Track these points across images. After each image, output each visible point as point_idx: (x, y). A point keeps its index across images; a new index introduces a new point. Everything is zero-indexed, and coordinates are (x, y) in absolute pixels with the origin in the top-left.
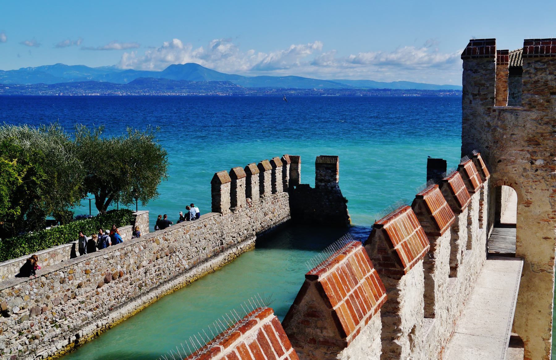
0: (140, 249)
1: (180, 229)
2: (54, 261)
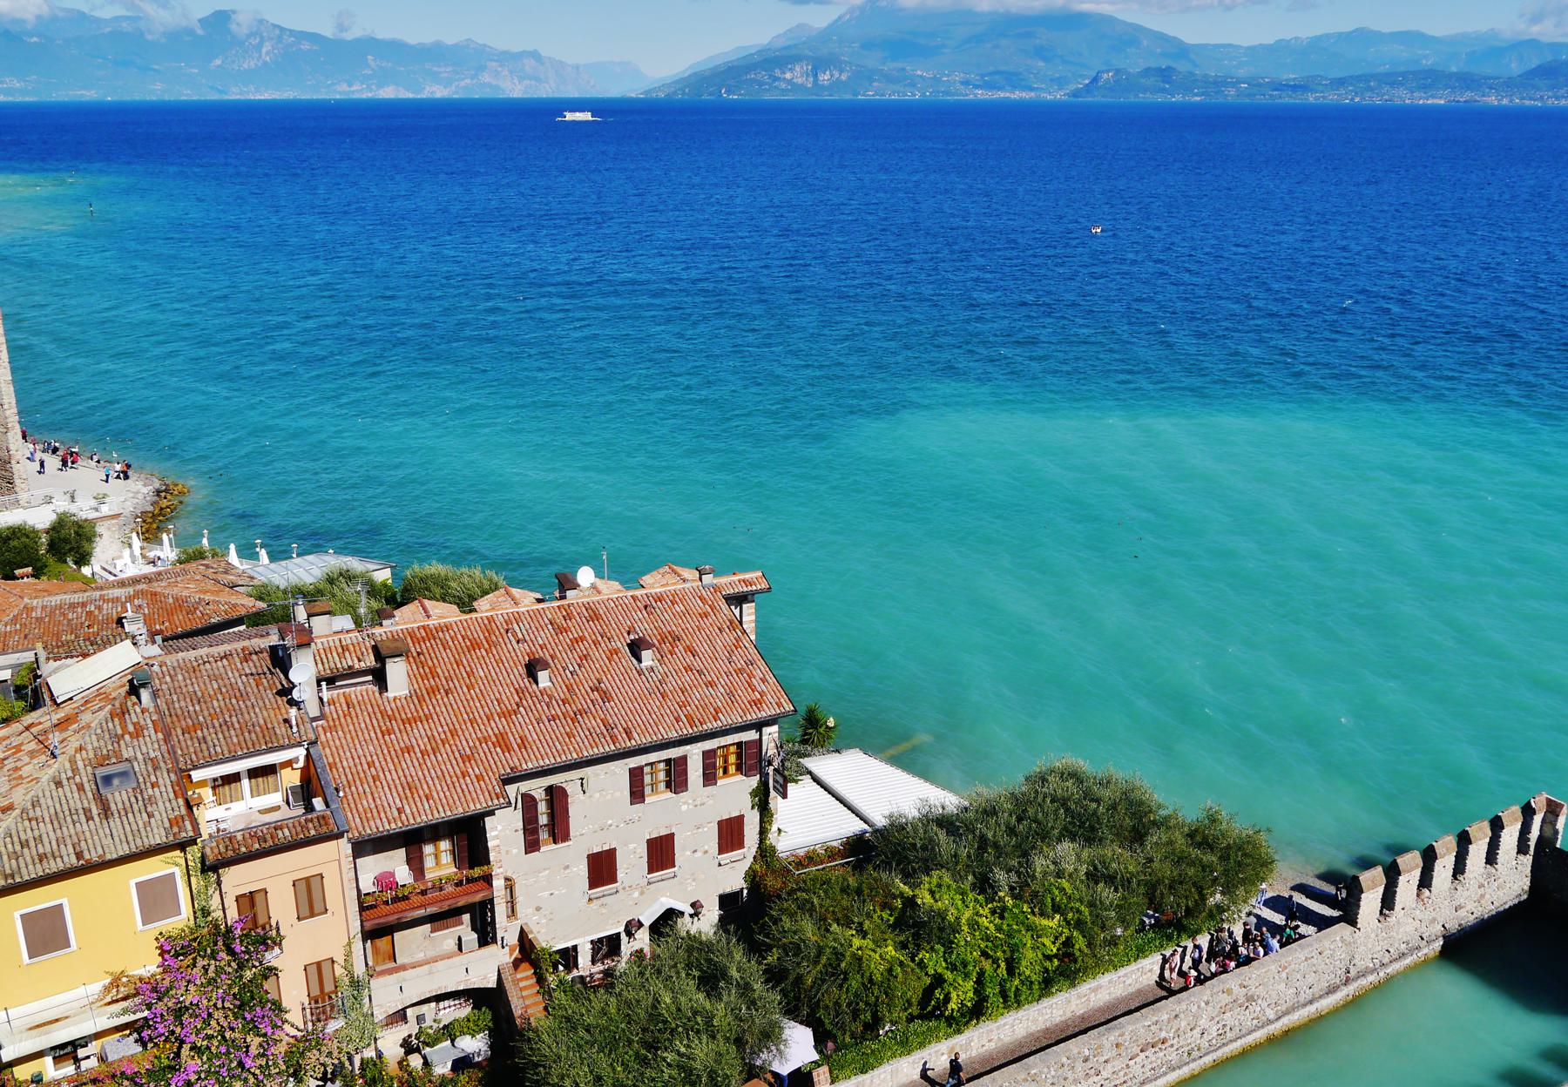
0: (1199, 1007)
1: (1273, 967)
2: (1096, 995)
